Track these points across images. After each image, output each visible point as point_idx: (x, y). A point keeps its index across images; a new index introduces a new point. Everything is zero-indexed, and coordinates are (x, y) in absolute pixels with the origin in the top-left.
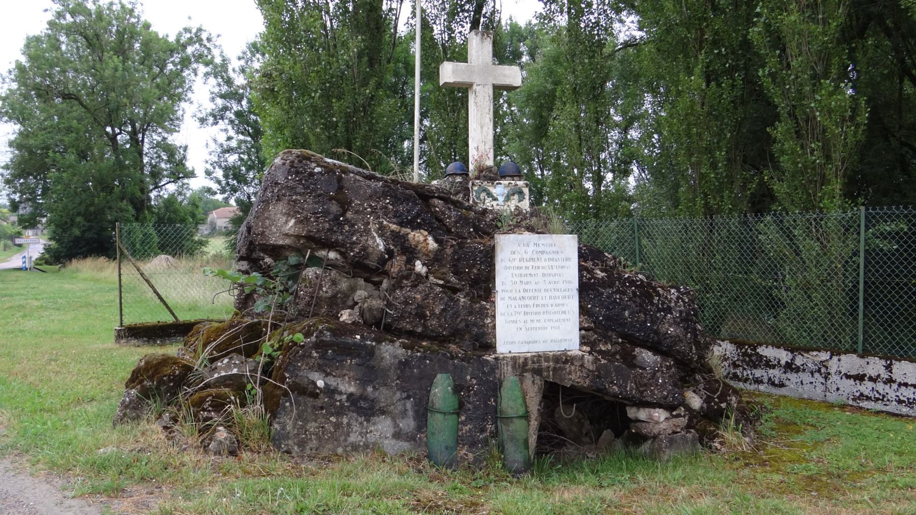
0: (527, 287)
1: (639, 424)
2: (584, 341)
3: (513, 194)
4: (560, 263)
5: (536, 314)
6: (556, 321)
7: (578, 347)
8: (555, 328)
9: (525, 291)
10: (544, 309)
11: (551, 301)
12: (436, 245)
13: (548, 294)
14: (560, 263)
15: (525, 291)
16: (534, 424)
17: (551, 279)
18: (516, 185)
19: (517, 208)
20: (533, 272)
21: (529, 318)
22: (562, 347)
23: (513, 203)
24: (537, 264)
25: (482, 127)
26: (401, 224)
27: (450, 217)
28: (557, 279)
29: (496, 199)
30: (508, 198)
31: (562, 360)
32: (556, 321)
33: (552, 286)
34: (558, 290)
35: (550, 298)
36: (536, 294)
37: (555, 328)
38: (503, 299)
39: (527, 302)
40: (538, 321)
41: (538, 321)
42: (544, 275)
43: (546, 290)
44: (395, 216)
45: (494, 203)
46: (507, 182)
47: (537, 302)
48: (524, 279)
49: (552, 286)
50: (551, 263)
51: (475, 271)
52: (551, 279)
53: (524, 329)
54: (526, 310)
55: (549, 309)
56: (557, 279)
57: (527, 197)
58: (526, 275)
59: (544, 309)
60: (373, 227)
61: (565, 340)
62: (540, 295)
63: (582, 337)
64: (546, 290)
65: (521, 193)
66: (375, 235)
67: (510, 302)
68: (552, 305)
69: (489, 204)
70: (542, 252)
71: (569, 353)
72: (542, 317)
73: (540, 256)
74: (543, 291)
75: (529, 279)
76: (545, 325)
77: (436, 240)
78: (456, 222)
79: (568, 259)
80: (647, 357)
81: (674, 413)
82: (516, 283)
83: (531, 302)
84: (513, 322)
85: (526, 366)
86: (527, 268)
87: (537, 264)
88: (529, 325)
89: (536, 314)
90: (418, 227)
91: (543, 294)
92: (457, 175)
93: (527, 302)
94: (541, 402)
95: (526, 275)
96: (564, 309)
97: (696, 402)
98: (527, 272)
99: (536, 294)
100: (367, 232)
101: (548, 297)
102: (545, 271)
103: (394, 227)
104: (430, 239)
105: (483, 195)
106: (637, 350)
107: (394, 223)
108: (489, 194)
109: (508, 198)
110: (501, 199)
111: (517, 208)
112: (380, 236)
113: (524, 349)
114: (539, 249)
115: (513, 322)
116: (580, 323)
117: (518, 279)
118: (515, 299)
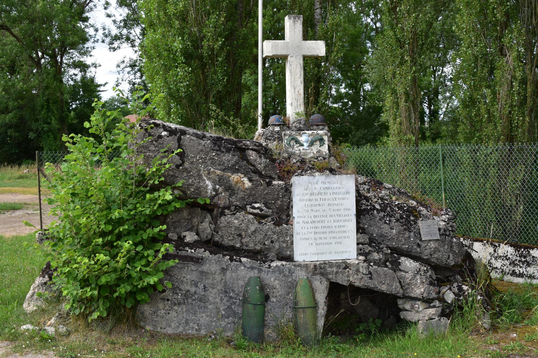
0: (317, 214)
1: (405, 312)
2: (360, 253)
3: (316, 141)
4: (341, 196)
5: (323, 233)
6: (339, 238)
7: (356, 257)
8: (338, 243)
9: (315, 216)
10: (330, 230)
11: (336, 224)
12: (250, 184)
13: (332, 219)
14: (341, 196)
15: (315, 216)
16: (322, 310)
17: (335, 207)
18: (318, 134)
19: (319, 151)
20: (321, 202)
21: (318, 236)
22: (344, 257)
23: (315, 148)
24: (324, 197)
25: (295, 89)
26: (224, 170)
27: (260, 164)
28: (339, 207)
29: (302, 145)
30: (312, 144)
31: (345, 265)
32: (339, 238)
33: (336, 213)
34: (340, 216)
35: (334, 221)
36: (323, 219)
37: (338, 243)
38: (298, 223)
39: (317, 225)
40: (325, 238)
41: (325, 238)
42: (329, 205)
43: (331, 216)
44: (219, 165)
45: (301, 148)
46: (310, 132)
47: (324, 225)
48: (315, 208)
49: (336, 213)
50: (335, 196)
51: (279, 202)
52: (335, 207)
53: (314, 244)
54: (316, 230)
55: (333, 229)
56: (339, 207)
57: (326, 143)
58: (315, 205)
59: (330, 230)
60: (203, 173)
61: (346, 252)
62: (326, 219)
63: (359, 250)
64: (331, 216)
65: (321, 140)
66: (205, 178)
67: (304, 225)
68: (335, 227)
69: (297, 149)
70: (328, 188)
71: (348, 261)
72: (327, 235)
73: (326, 191)
74: (328, 216)
75: (318, 208)
76: (331, 241)
77: (250, 180)
78: (265, 167)
79: (348, 193)
80: (407, 263)
81: (432, 305)
82: (308, 211)
83: (319, 225)
84: (306, 239)
85: (319, 269)
86: (316, 200)
87: (324, 197)
88: (319, 241)
89: (323, 233)
90: (237, 171)
91: (329, 218)
92: (276, 125)
93: (317, 225)
94: (327, 297)
95: (315, 205)
96: (344, 229)
97: (450, 297)
98: (317, 203)
99: (323, 219)
100: (200, 176)
101: (332, 221)
102: (330, 202)
103: (218, 172)
104: (246, 180)
105: (292, 143)
106: (403, 259)
107: (220, 170)
108: (297, 142)
109: (312, 144)
110: (306, 145)
111: (319, 151)
112: (209, 179)
113: (315, 258)
114: (326, 186)
115: (306, 239)
116: (357, 239)
117: (310, 209)
118: (307, 223)
